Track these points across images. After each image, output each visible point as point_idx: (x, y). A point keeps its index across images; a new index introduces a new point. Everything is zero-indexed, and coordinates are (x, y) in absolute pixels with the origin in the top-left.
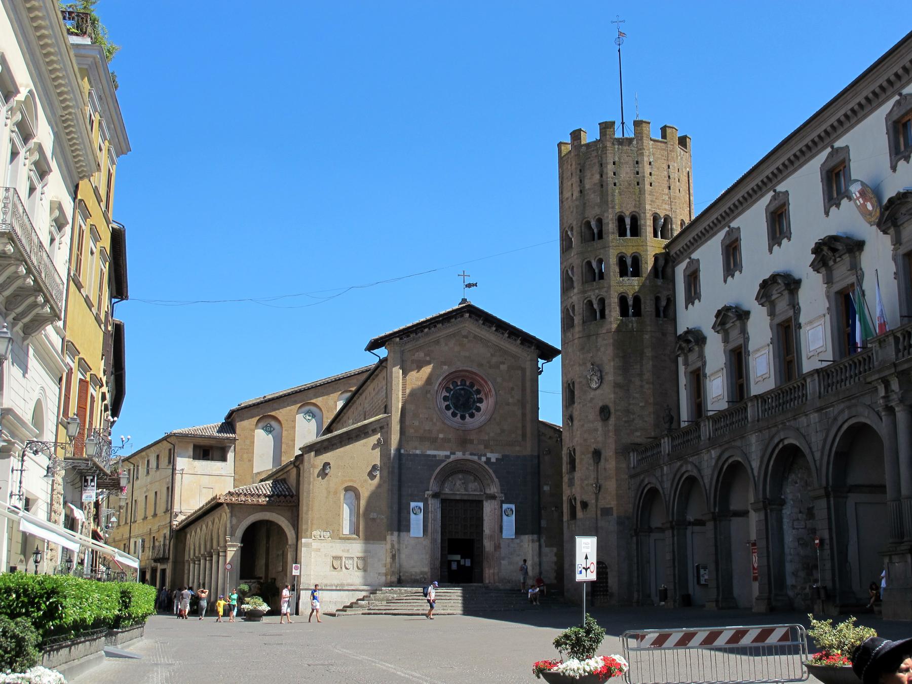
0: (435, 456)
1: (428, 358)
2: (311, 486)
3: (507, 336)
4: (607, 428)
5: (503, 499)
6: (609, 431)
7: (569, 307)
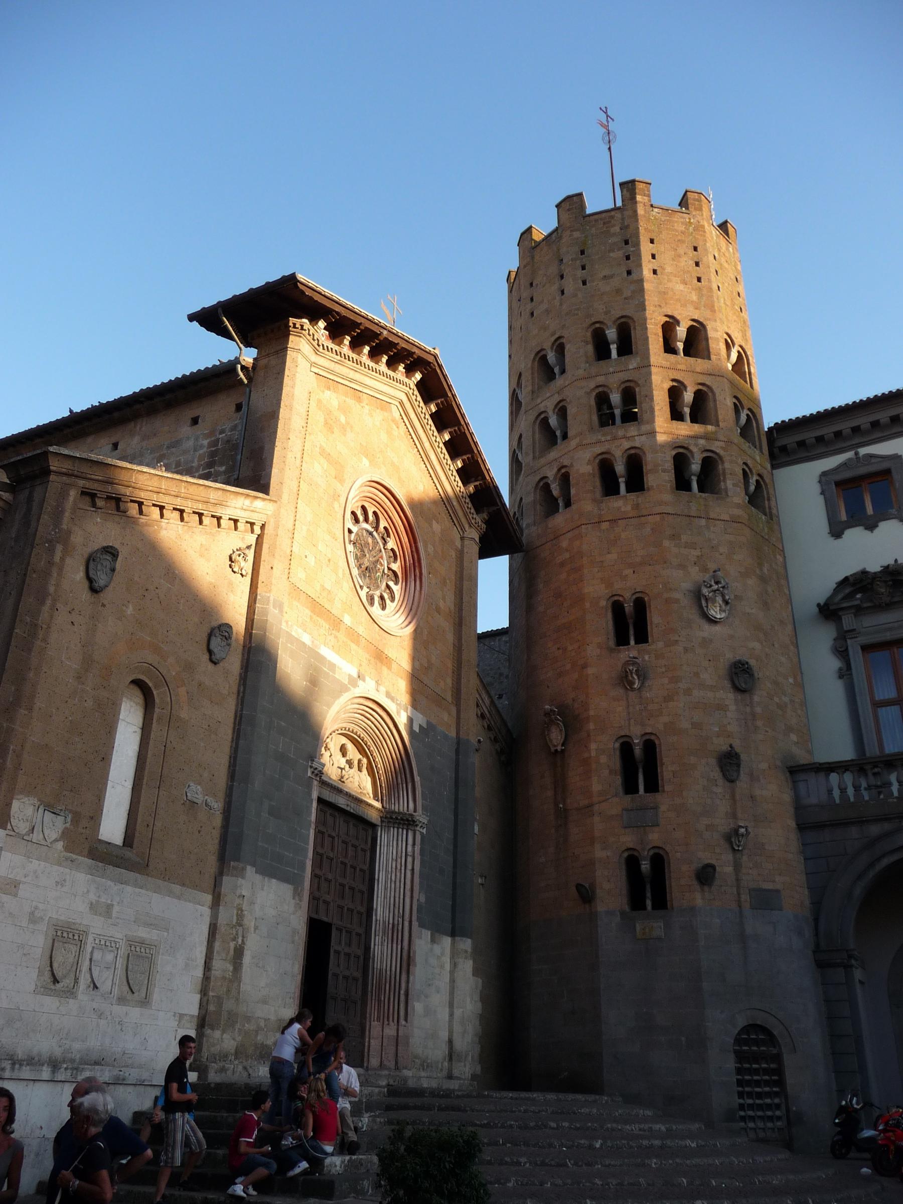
1: (343, 419)
2: (46, 608)
3: (460, 466)
5: (424, 831)
6: (754, 715)
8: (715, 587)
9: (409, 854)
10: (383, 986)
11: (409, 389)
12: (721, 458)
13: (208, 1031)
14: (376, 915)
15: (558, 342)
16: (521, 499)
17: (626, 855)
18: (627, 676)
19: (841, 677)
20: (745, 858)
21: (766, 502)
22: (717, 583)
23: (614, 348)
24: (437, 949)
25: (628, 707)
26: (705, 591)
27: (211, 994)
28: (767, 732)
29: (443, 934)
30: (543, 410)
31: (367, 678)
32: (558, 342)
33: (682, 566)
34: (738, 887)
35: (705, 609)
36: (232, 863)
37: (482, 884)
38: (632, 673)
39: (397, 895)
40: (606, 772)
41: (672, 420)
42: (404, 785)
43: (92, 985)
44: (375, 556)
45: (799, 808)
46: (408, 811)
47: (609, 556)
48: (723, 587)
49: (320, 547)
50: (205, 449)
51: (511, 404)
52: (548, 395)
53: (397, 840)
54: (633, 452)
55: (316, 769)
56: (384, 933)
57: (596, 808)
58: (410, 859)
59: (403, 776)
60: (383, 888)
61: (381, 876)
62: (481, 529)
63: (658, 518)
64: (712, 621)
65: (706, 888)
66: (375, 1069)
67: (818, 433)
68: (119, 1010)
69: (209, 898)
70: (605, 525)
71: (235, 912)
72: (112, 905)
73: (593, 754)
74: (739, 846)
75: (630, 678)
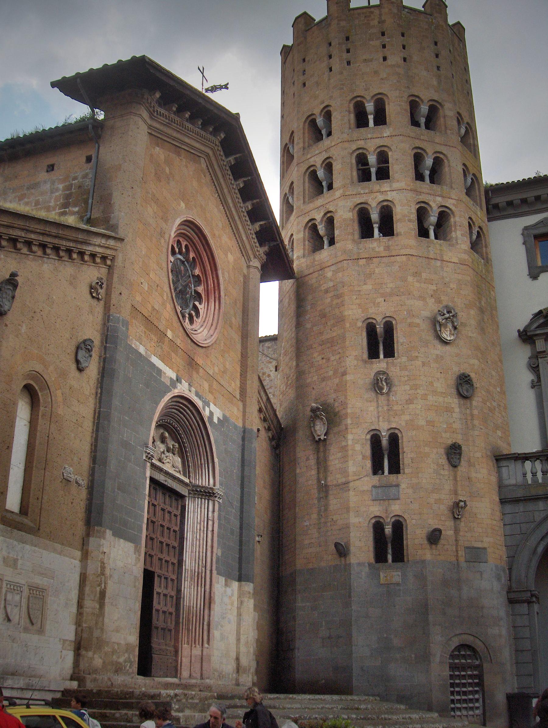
0: (159, 371)
4: (468, 411)
6: (472, 415)
7: (374, 204)
8: (447, 315)
9: (210, 519)
10: (191, 619)
11: (214, 145)
12: (453, 213)
13: (83, 652)
14: (185, 565)
15: (326, 109)
16: (292, 235)
17: (373, 521)
18: (378, 383)
19: (533, 387)
20: (462, 524)
21: (484, 249)
22: (449, 312)
23: (371, 118)
24: (229, 590)
25: (378, 407)
26: (440, 318)
27: (84, 625)
28: (482, 429)
29: (233, 580)
30: (312, 164)
31: (183, 381)
32: (326, 109)
33: (422, 298)
34: (457, 545)
35: (439, 332)
36: (96, 527)
37: (259, 542)
38: (382, 381)
39: (201, 550)
40: (360, 457)
41: (416, 180)
42: (206, 465)
43: (7, 619)
44: (186, 281)
45: (501, 486)
46: (209, 485)
47: (365, 287)
48: (453, 316)
49: (152, 275)
50: (60, 192)
51: (282, 156)
52: (317, 152)
53: (201, 508)
54: (385, 203)
55: (149, 453)
56: (191, 578)
57: (351, 484)
58: (210, 523)
59: (206, 458)
60: (190, 545)
61: (189, 536)
62: (263, 259)
63: (404, 258)
64: (445, 342)
65: (434, 546)
66: (185, 679)
67: (524, 196)
68: (23, 636)
69: (78, 554)
70: (362, 262)
71: (100, 565)
72: (18, 559)
73: (350, 442)
74: (458, 516)
75: (381, 385)
